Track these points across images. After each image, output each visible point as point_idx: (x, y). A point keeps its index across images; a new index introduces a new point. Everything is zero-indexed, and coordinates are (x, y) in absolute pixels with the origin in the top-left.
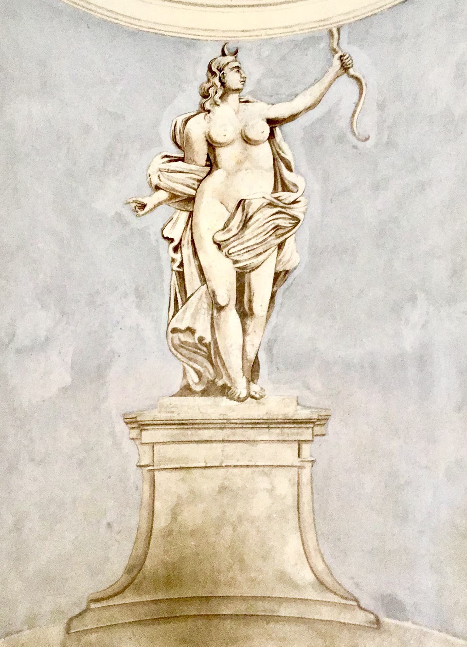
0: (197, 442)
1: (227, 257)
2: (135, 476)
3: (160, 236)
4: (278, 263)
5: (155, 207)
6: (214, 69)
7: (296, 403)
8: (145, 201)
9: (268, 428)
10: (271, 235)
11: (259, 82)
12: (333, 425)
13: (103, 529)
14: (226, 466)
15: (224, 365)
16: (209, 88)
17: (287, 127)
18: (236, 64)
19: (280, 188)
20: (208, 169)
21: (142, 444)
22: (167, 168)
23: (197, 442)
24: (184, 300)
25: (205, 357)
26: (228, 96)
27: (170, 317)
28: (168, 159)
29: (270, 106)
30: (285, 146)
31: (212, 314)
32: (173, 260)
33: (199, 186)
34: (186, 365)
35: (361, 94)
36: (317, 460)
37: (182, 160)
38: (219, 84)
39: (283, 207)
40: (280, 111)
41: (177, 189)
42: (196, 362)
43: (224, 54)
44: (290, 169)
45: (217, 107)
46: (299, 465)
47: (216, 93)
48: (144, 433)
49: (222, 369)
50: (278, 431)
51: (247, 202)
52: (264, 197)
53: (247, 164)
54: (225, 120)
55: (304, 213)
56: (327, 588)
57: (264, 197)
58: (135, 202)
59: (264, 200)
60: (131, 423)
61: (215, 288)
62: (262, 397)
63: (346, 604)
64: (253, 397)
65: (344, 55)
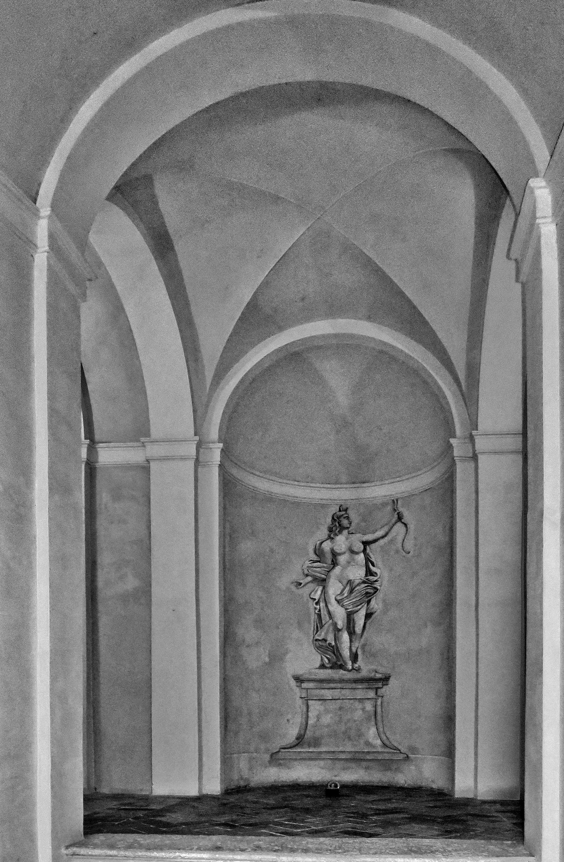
2: (299, 702)
4: (367, 610)
6: (336, 518)
8: (301, 581)
11: (358, 524)
13: (286, 721)
15: (341, 656)
17: (373, 546)
20: (332, 566)
30: (370, 554)
32: (316, 608)
35: (407, 530)
37: (319, 562)
38: (338, 525)
40: (369, 537)
43: (340, 511)
44: (373, 565)
50: (367, 684)
54: (341, 542)
64: (354, 669)
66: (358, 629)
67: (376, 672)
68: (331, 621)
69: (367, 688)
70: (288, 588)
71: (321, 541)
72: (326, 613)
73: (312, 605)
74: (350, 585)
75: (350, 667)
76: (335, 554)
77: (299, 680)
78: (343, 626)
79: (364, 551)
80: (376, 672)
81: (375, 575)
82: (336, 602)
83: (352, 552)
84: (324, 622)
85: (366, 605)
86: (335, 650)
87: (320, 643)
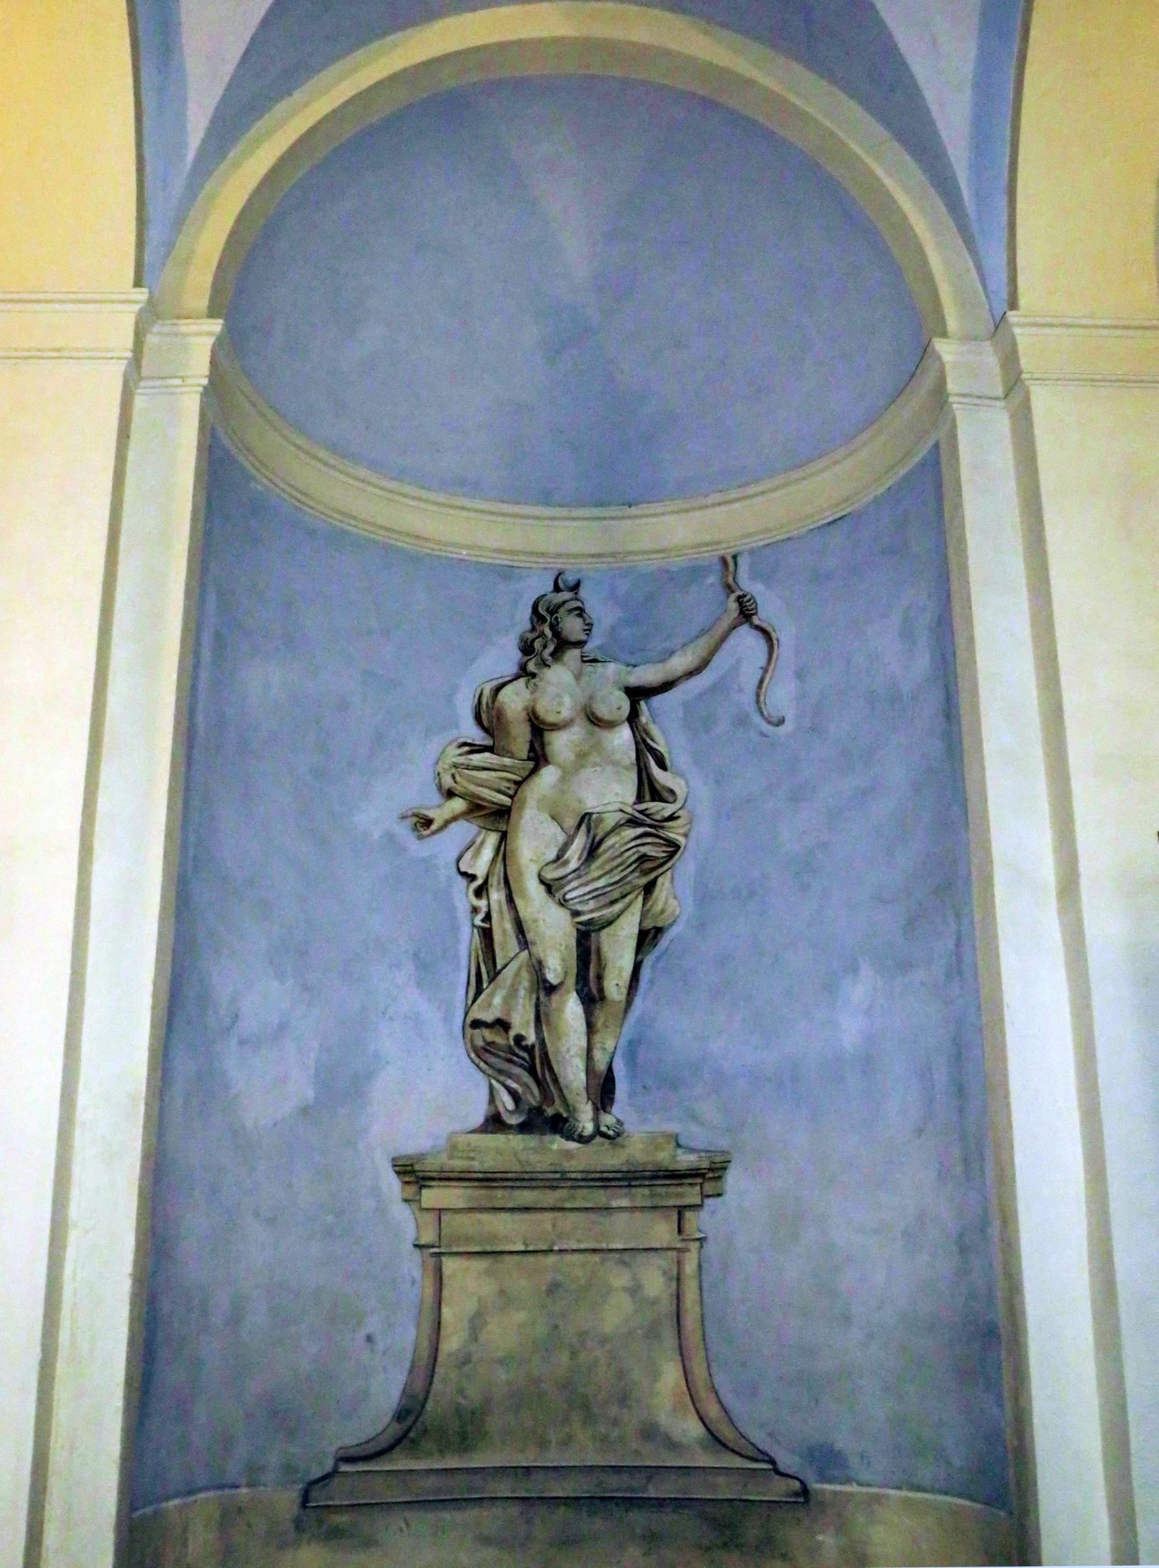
0: (512, 1210)
1: (563, 905)
2: (412, 1266)
3: (455, 870)
4: (644, 915)
5: (447, 823)
7: (674, 1144)
8: (431, 814)
9: (630, 1186)
10: (633, 871)
11: (613, 628)
12: (733, 1179)
14: (561, 1251)
15: (556, 1080)
16: (533, 641)
17: (656, 700)
18: (579, 604)
19: (648, 797)
20: (531, 765)
21: (422, 1209)
22: (466, 762)
23: (512, 1210)
24: (492, 973)
25: (525, 1069)
26: (563, 652)
27: (470, 1002)
28: (467, 749)
29: (630, 669)
30: (655, 731)
31: (538, 999)
32: (475, 910)
33: (516, 793)
34: (494, 1082)
36: (710, 1236)
38: (548, 633)
39: (650, 826)
40: (648, 675)
41: (483, 795)
42: (510, 1076)
43: (557, 589)
44: (662, 765)
45: (546, 670)
46: (679, 1246)
47: (545, 647)
48: (424, 1191)
49: (552, 1088)
50: (646, 1191)
51: (594, 816)
52: (621, 810)
53: (594, 757)
54: (559, 688)
55: (686, 835)
56: (724, 1445)
57: (621, 810)
58: (415, 815)
59: (620, 815)
60: (405, 1173)
61: (542, 955)
62: (618, 1135)
63: (755, 1470)
64: (604, 1135)
65: (744, 596)
66: (615, 985)
67: (679, 1146)
68: (525, 953)
69: (642, 1209)
70: (390, 837)
71: (495, 683)
72: (509, 926)
73: (463, 896)
74: (589, 831)
75: (589, 1128)
76: (539, 728)
77: (413, 1174)
78: (566, 973)
79: (633, 718)
80: (679, 1146)
81: (671, 799)
82: (542, 888)
83: (595, 721)
84: (500, 963)
85: (640, 899)
86: (537, 1062)
87: (488, 1035)
